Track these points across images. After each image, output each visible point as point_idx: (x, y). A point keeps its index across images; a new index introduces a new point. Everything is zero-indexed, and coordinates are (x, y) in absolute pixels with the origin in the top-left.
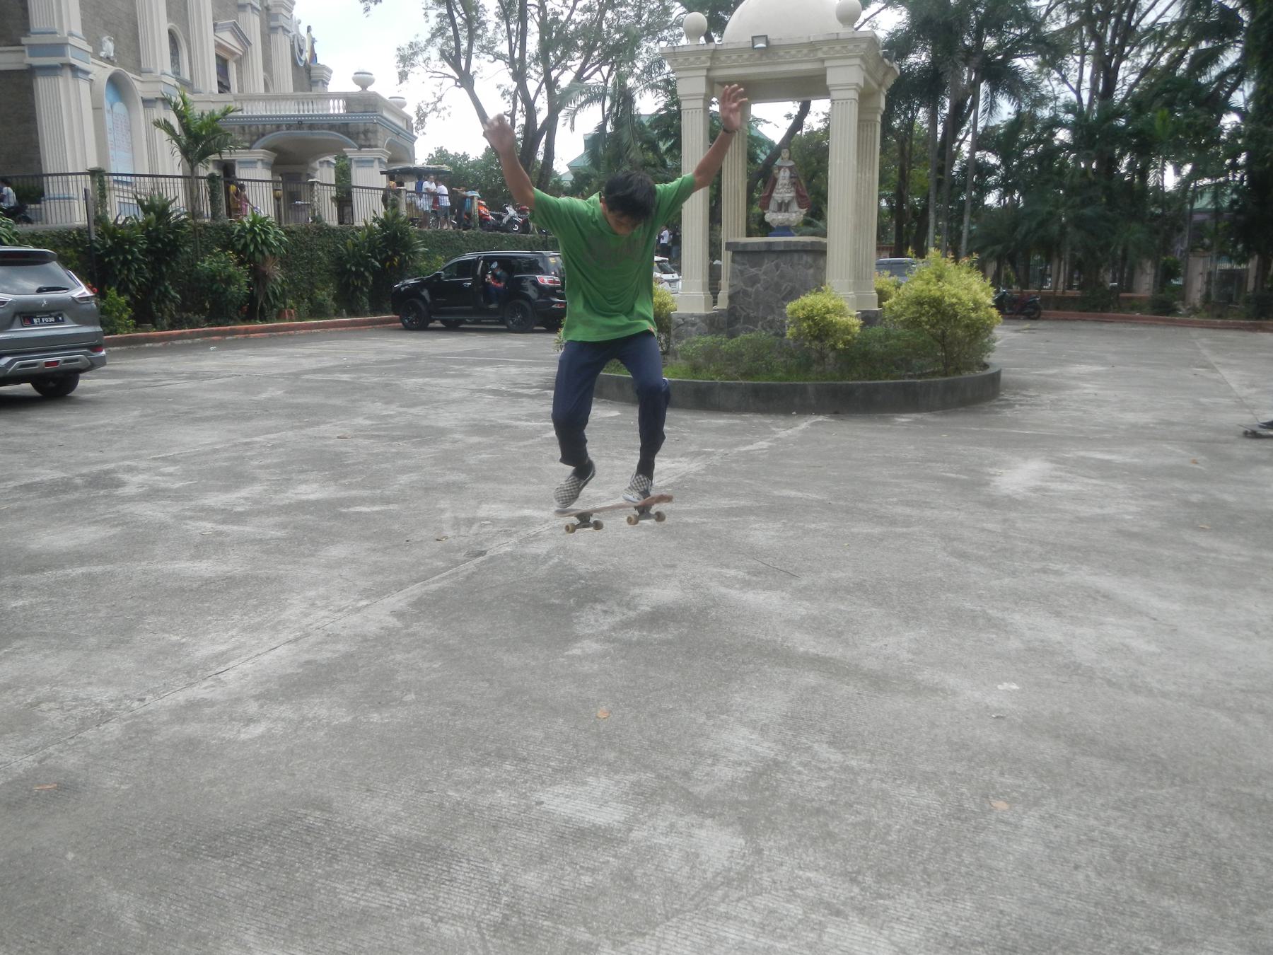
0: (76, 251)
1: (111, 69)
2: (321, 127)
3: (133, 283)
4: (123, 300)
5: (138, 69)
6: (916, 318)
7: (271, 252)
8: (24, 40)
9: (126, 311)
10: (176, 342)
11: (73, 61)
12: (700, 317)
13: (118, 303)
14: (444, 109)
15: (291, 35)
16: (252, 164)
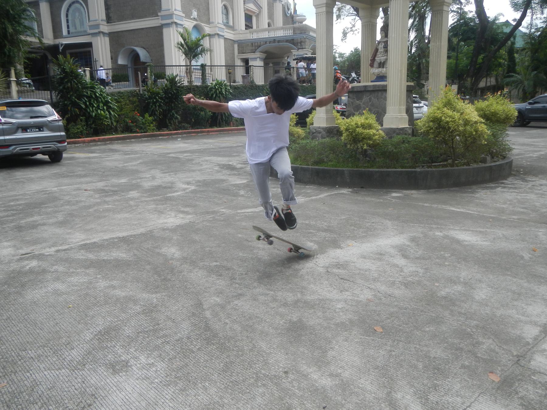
0: (137, 99)
1: (195, 23)
2: (282, 41)
3: (157, 111)
4: (150, 118)
5: (208, 22)
6: (428, 130)
7: (224, 97)
8: (159, 14)
9: (152, 123)
10: (174, 136)
11: (176, 21)
12: (323, 128)
13: (149, 120)
14: (356, 30)
15: (283, 3)
16: (255, 59)
